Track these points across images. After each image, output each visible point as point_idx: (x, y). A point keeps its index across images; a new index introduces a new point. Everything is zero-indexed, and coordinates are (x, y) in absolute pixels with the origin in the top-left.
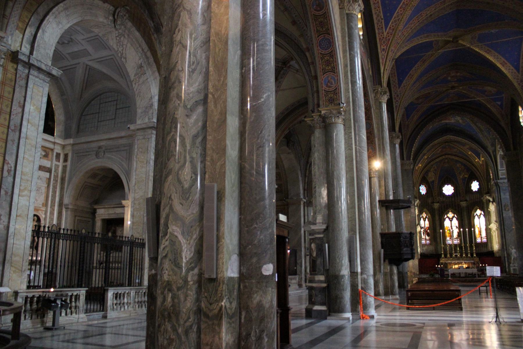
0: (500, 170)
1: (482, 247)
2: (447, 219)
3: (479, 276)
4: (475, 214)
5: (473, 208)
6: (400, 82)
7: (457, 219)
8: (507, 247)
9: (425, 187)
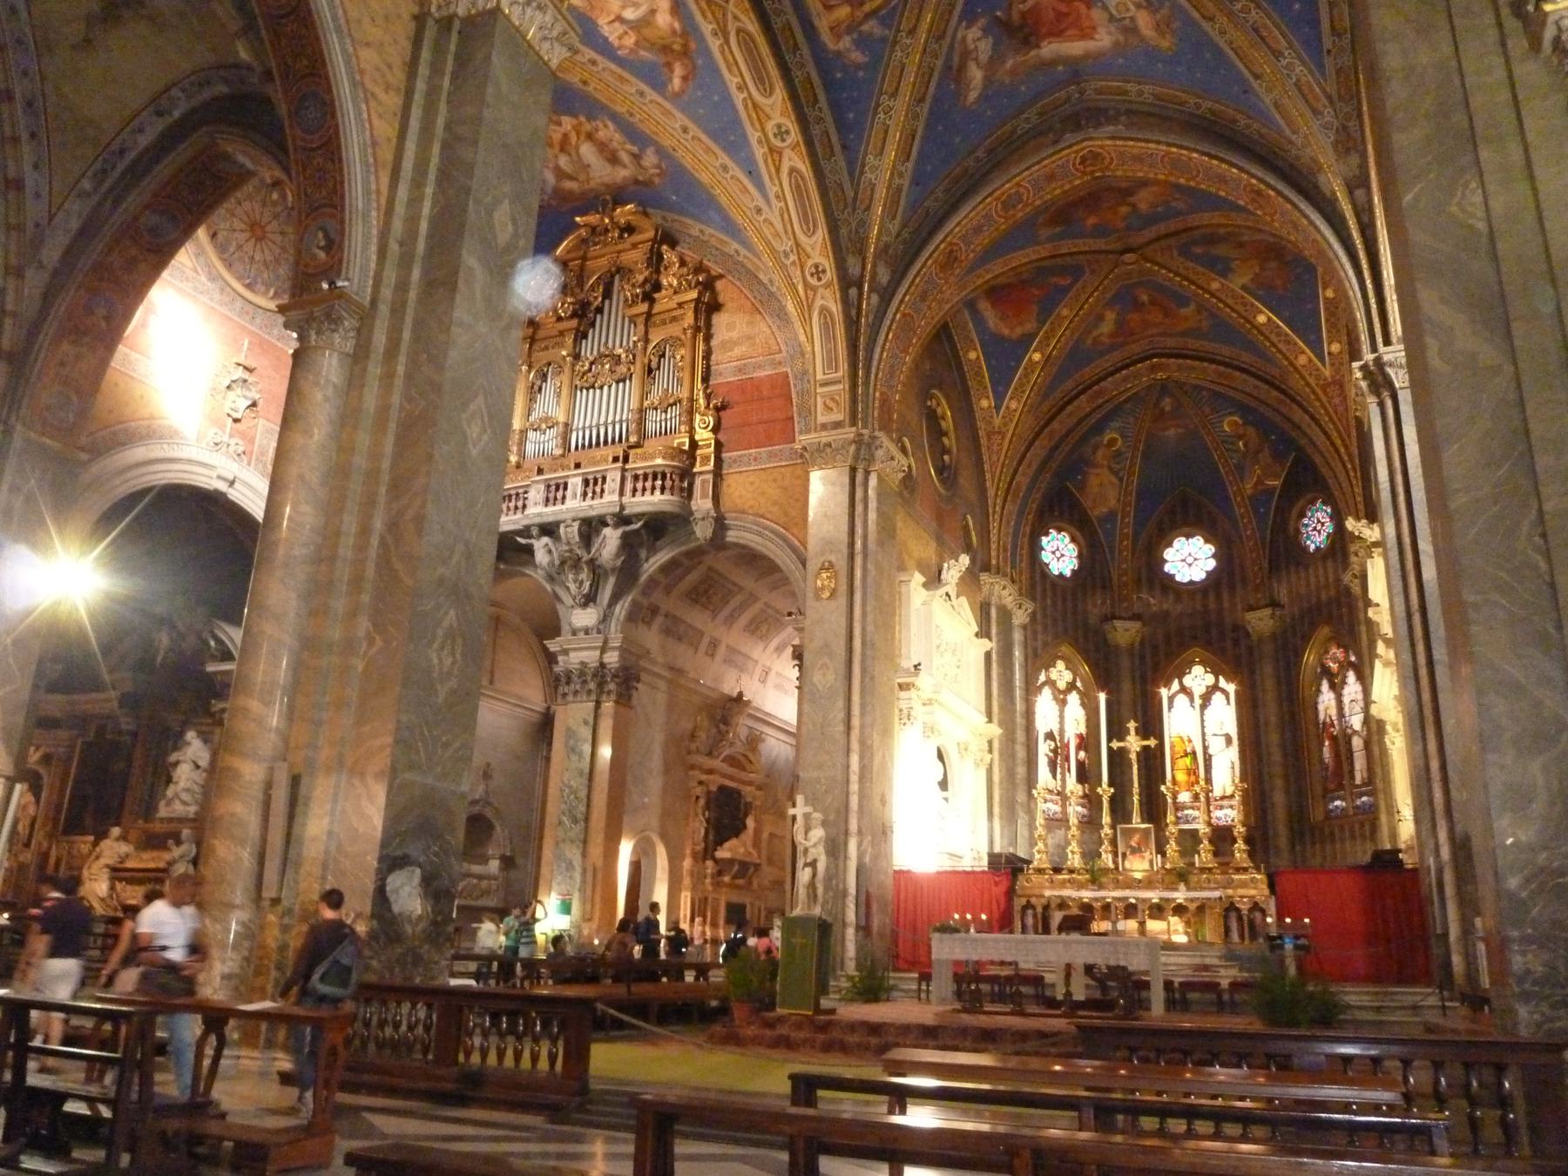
1: (1353, 837)
5: (1306, 639)
9: (1073, 540)
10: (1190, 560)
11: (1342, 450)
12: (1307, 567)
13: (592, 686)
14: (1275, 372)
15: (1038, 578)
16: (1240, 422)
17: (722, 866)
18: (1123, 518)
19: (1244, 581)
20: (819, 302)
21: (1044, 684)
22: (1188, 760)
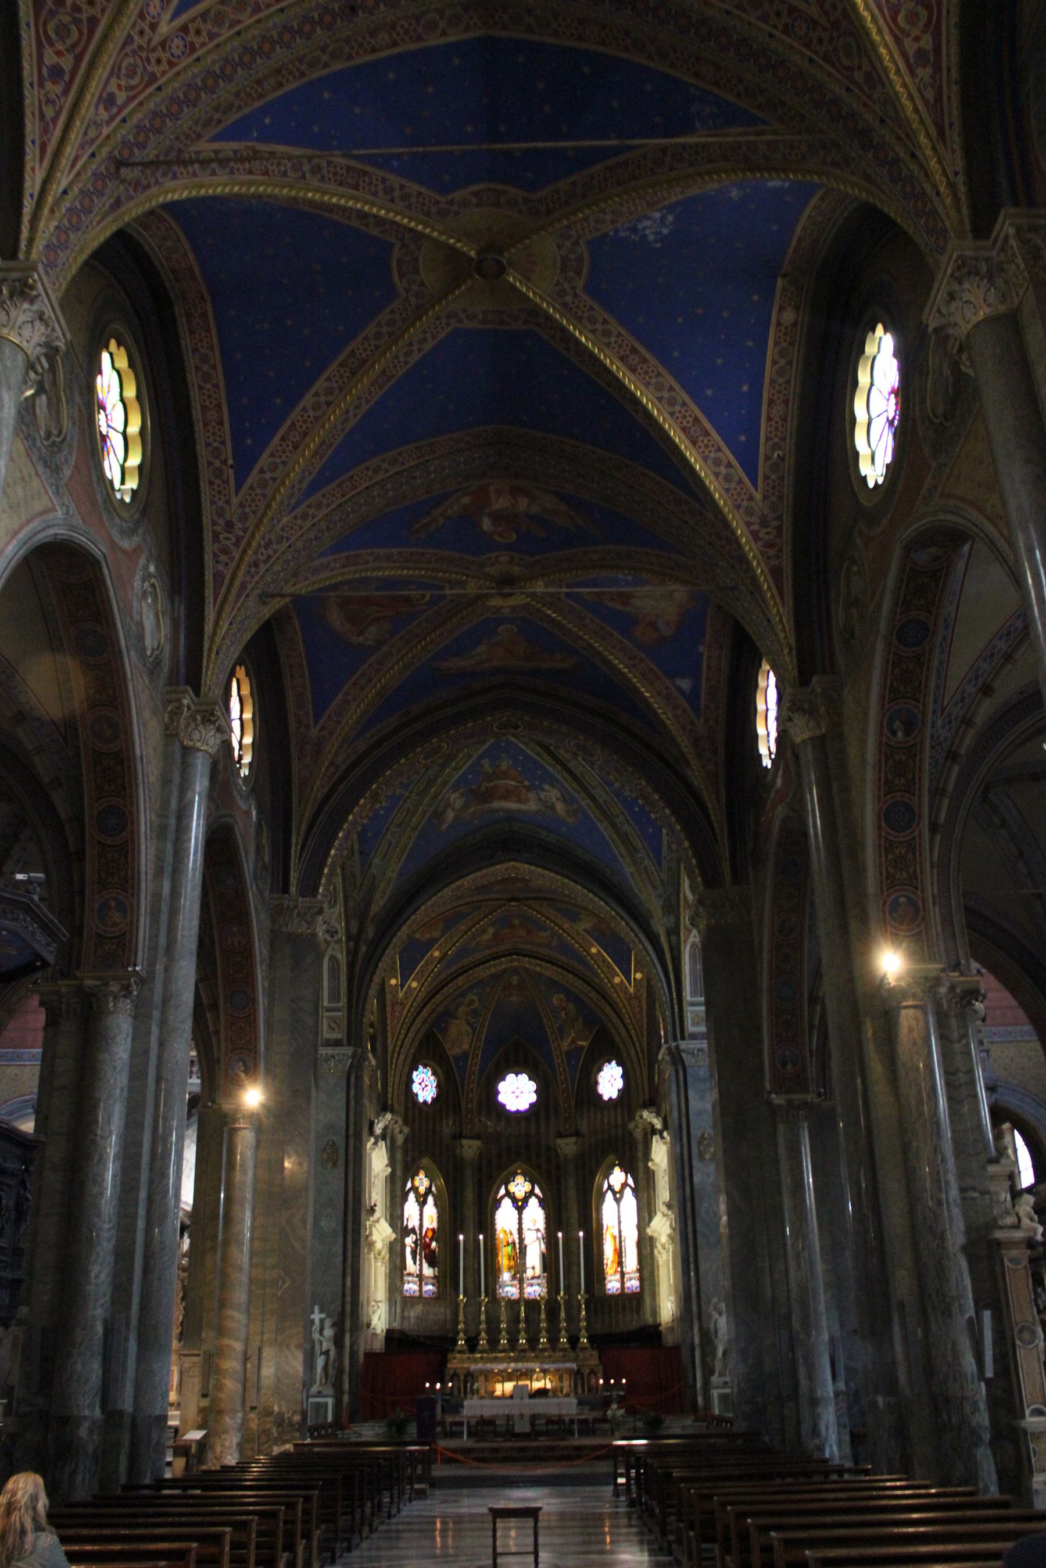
0: (692, 1004)
1: (624, 1309)
2: (507, 1203)
3: (587, 1428)
4: (606, 1186)
5: (598, 1164)
6: (244, 463)
8: (703, 1307)
9: (434, 1073)
10: (518, 1093)
11: (637, 1044)
14: (597, 980)
15: (410, 1105)
18: (473, 1059)
20: (330, 952)
21: (410, 1190)
22: (509, 1248)
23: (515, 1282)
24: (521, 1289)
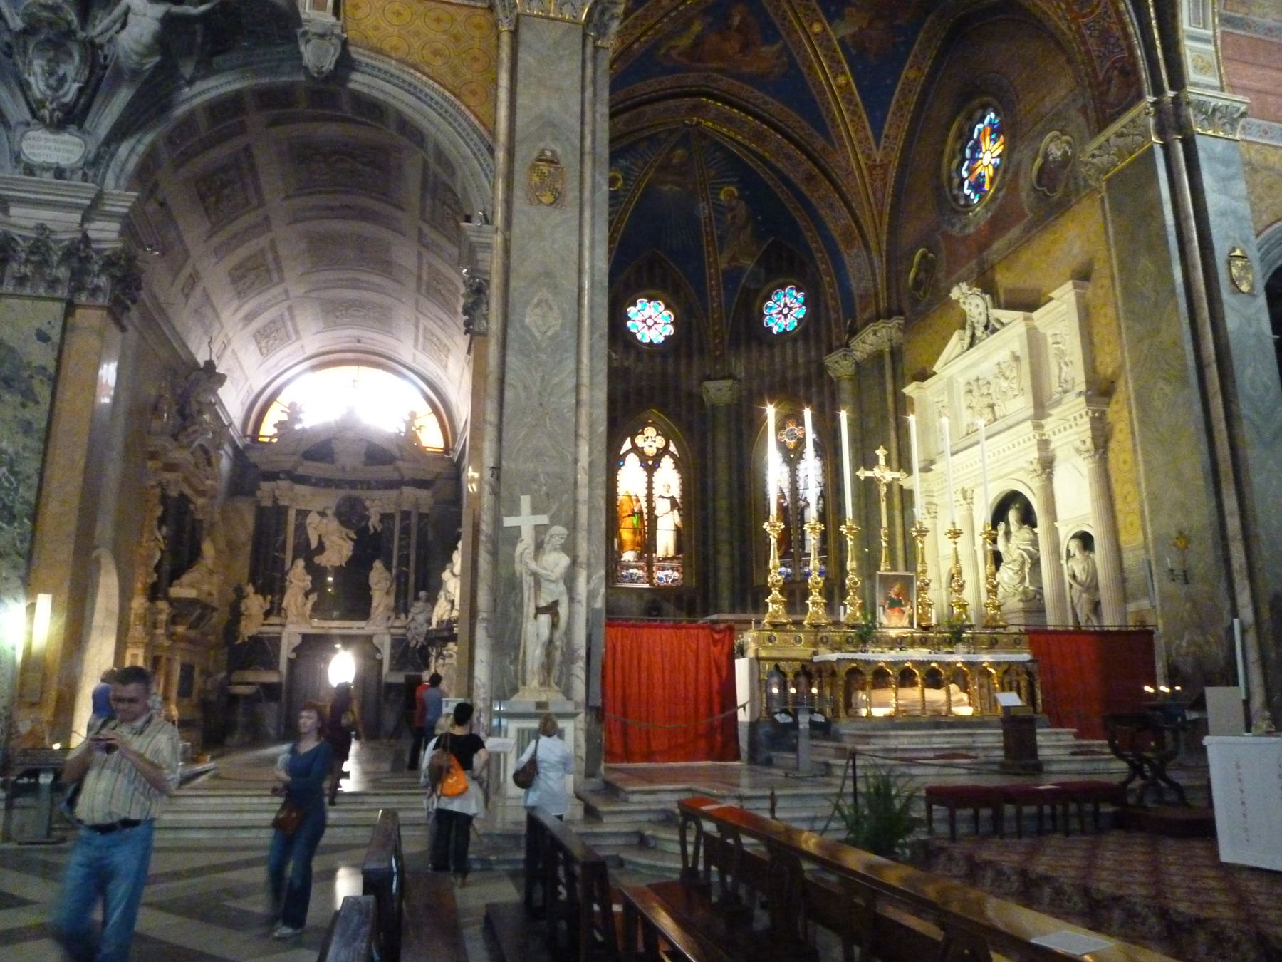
2: (632, 461)
7: (677, 467)
10: (650, 322)
12: (771, 346)
13: (62, 273)
14: (819, 142)
16: (736, 194)
17: (181, 609)
19: (701, 351)
22: (635, 520)
23: (642, 564)
24: (650, 573)
